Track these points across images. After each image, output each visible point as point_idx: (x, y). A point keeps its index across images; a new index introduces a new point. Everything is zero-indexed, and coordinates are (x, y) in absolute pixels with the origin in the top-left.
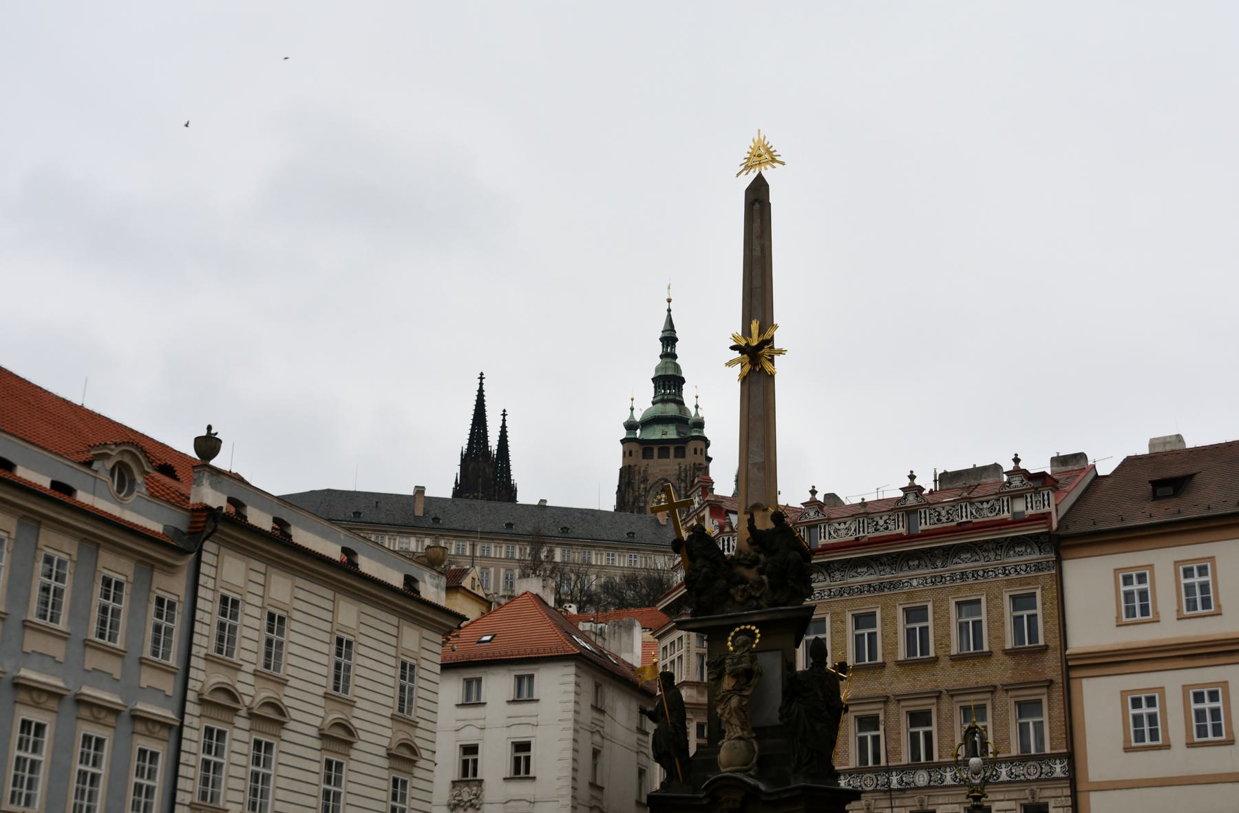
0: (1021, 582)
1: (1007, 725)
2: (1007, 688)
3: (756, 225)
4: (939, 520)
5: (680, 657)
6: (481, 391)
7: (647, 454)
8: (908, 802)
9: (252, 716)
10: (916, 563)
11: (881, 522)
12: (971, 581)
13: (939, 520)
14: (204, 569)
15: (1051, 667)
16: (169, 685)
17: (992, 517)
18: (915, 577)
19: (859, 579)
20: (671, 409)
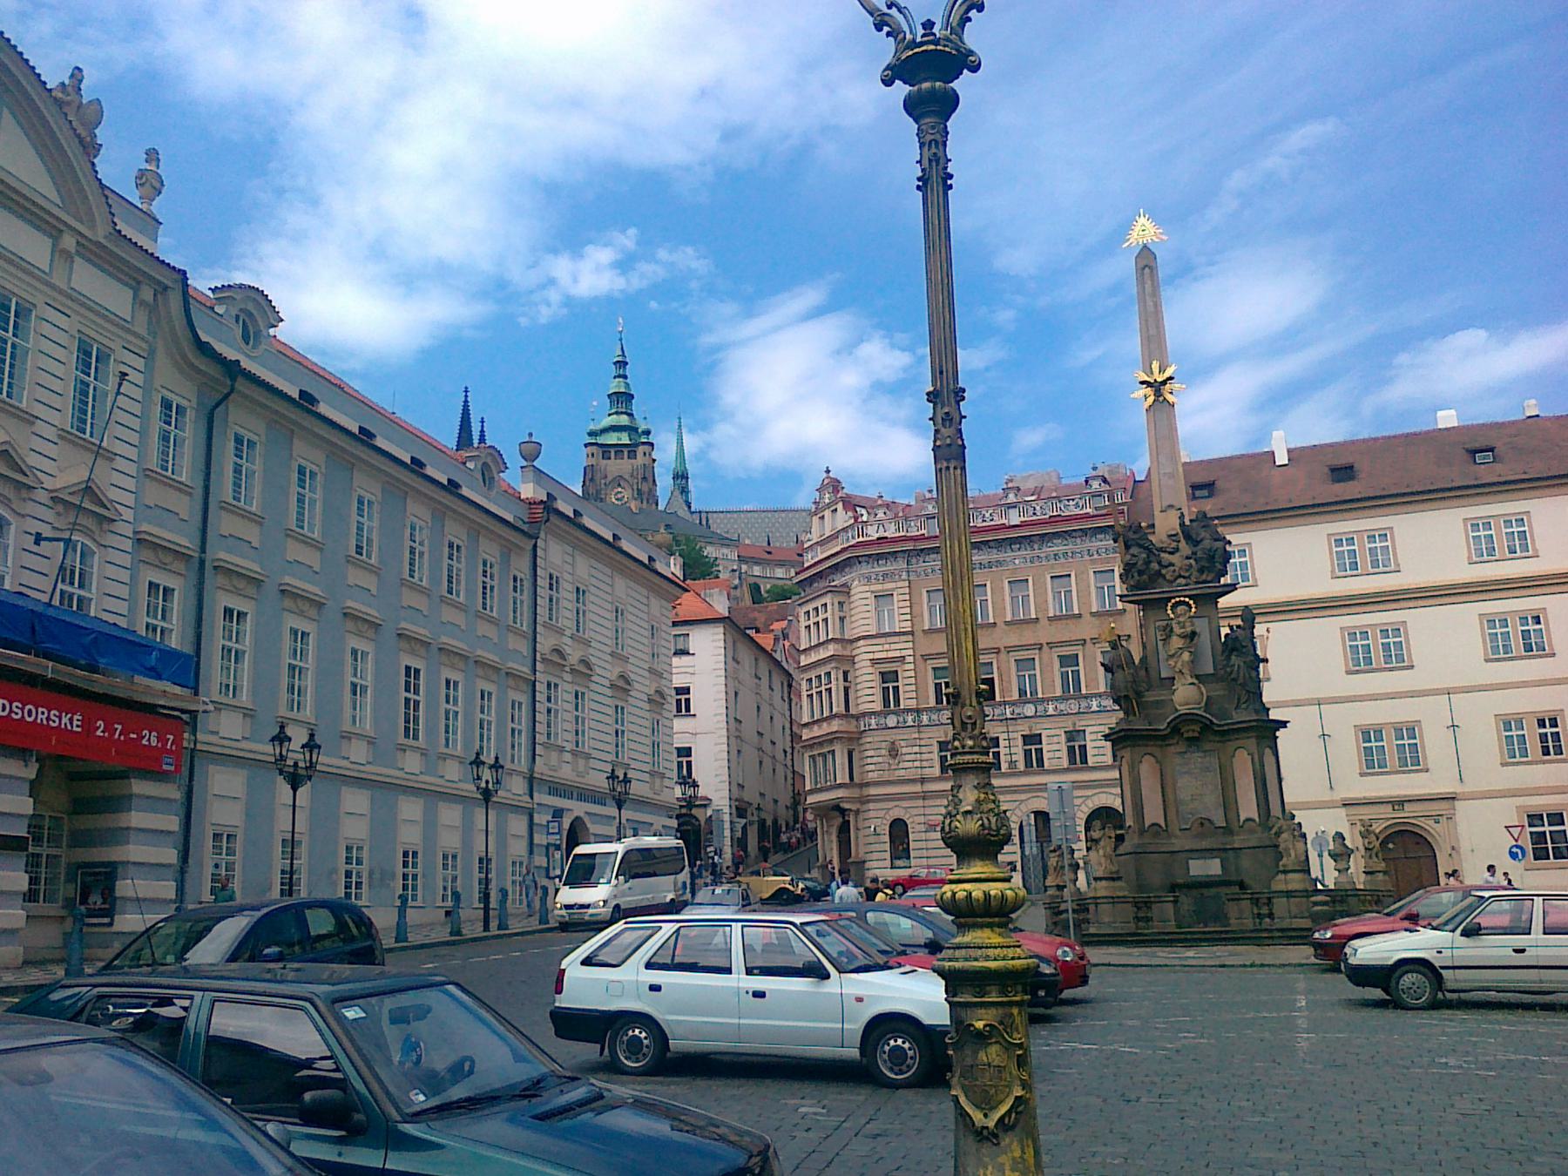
3: (1148, 286)
5: (826, 620)
6: (466, 401)
7: (606, 456)
9: (573, 671)
14: (540, 552)
16: (524, 647)
18: (1017, 558)
20: (624, 420)
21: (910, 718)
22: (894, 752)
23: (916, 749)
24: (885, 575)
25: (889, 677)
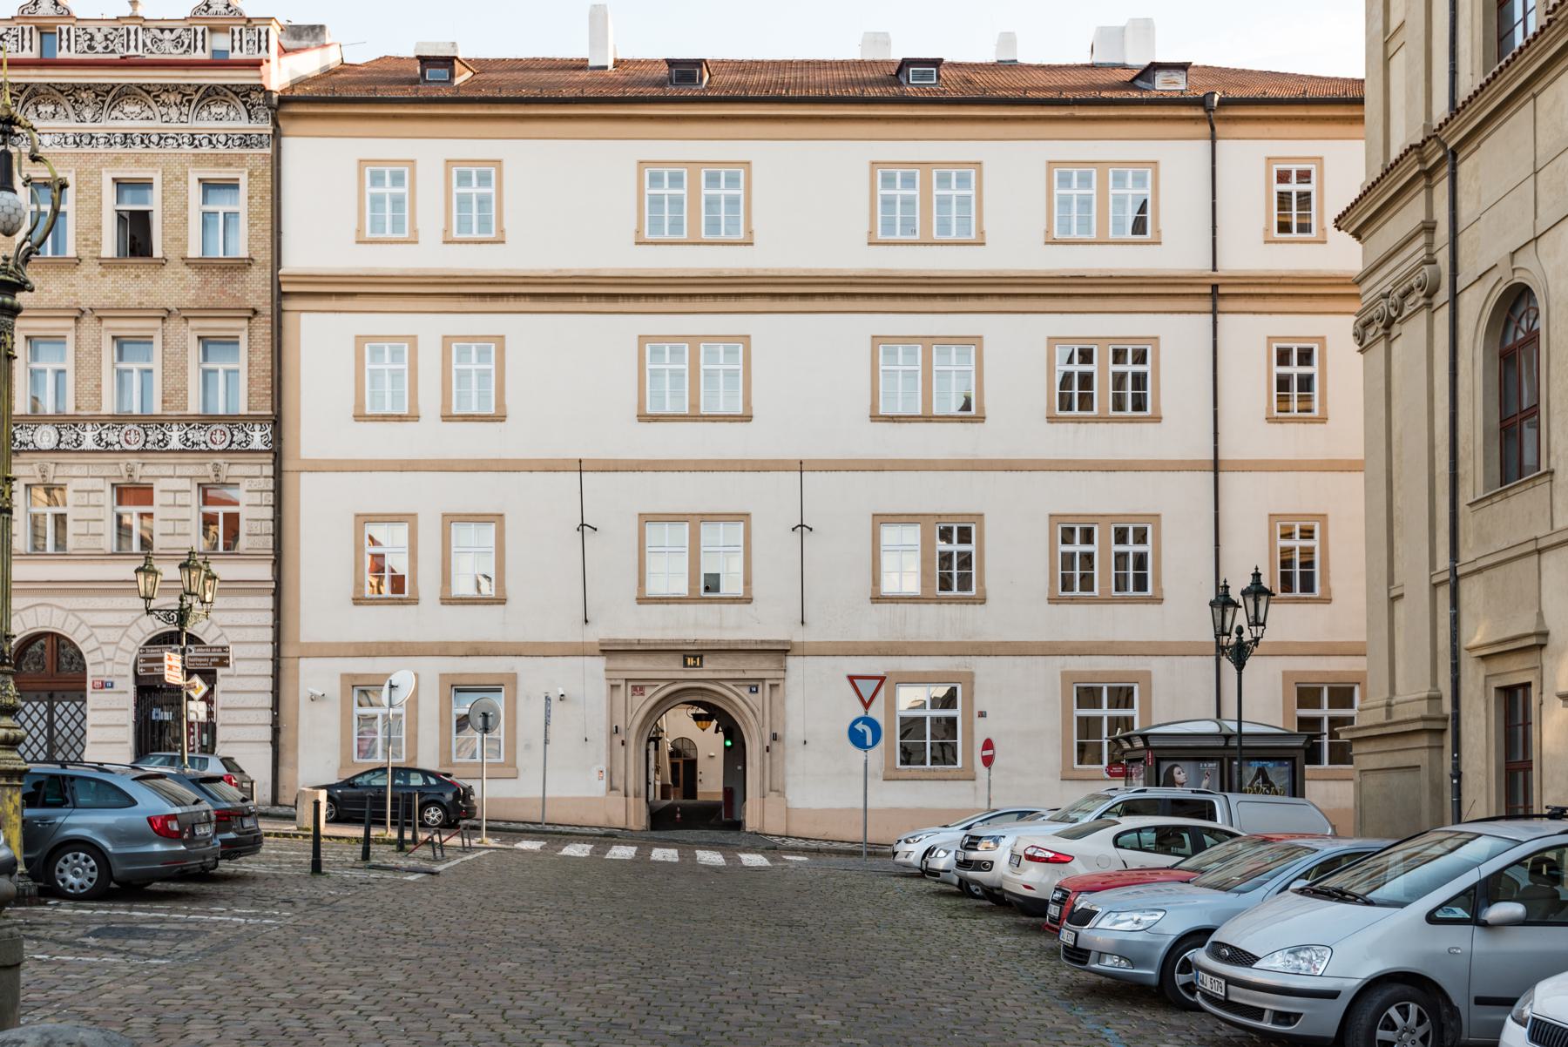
0: (219, 161)
1: (184, 369)
2: (186, 315)
4: (91, 47)
10: (51, 108)
12: (139, 148)
13: (91, 47)
15: (256, 289)
17: (177, 54)
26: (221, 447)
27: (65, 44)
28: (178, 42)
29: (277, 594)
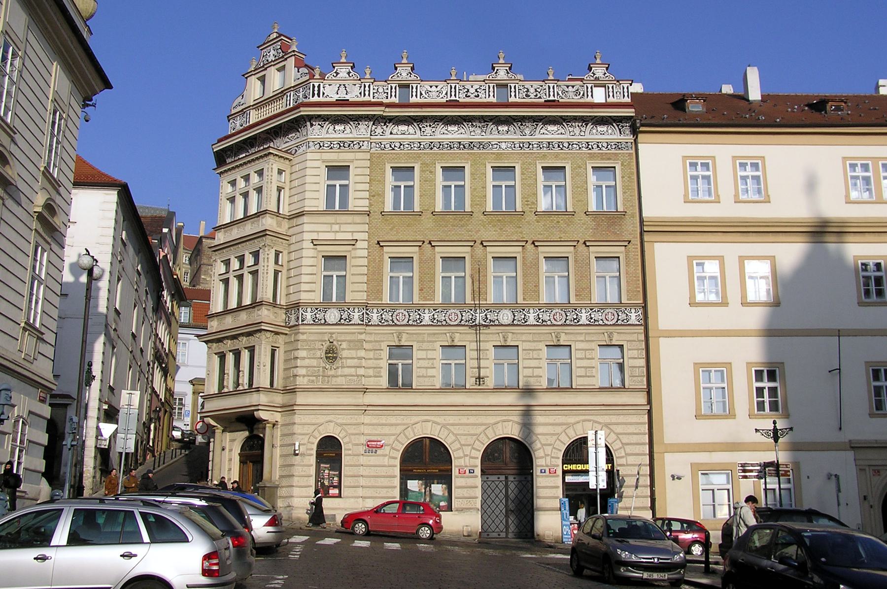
0: (603, 157)
4: (527, 96)
8: (490, 337)
11: (472, 90)
12: (557, 150)
13: (527, 96)
17: (576, 99)
19: (450, 136)
21: (356, 316)
22: (331, 355)
23: (362, 353)
24: (342, 144)
25: (335, 260)
26: (611, 323)
27: (513, 94)
28: (577, 93)
29: (650, 412)
